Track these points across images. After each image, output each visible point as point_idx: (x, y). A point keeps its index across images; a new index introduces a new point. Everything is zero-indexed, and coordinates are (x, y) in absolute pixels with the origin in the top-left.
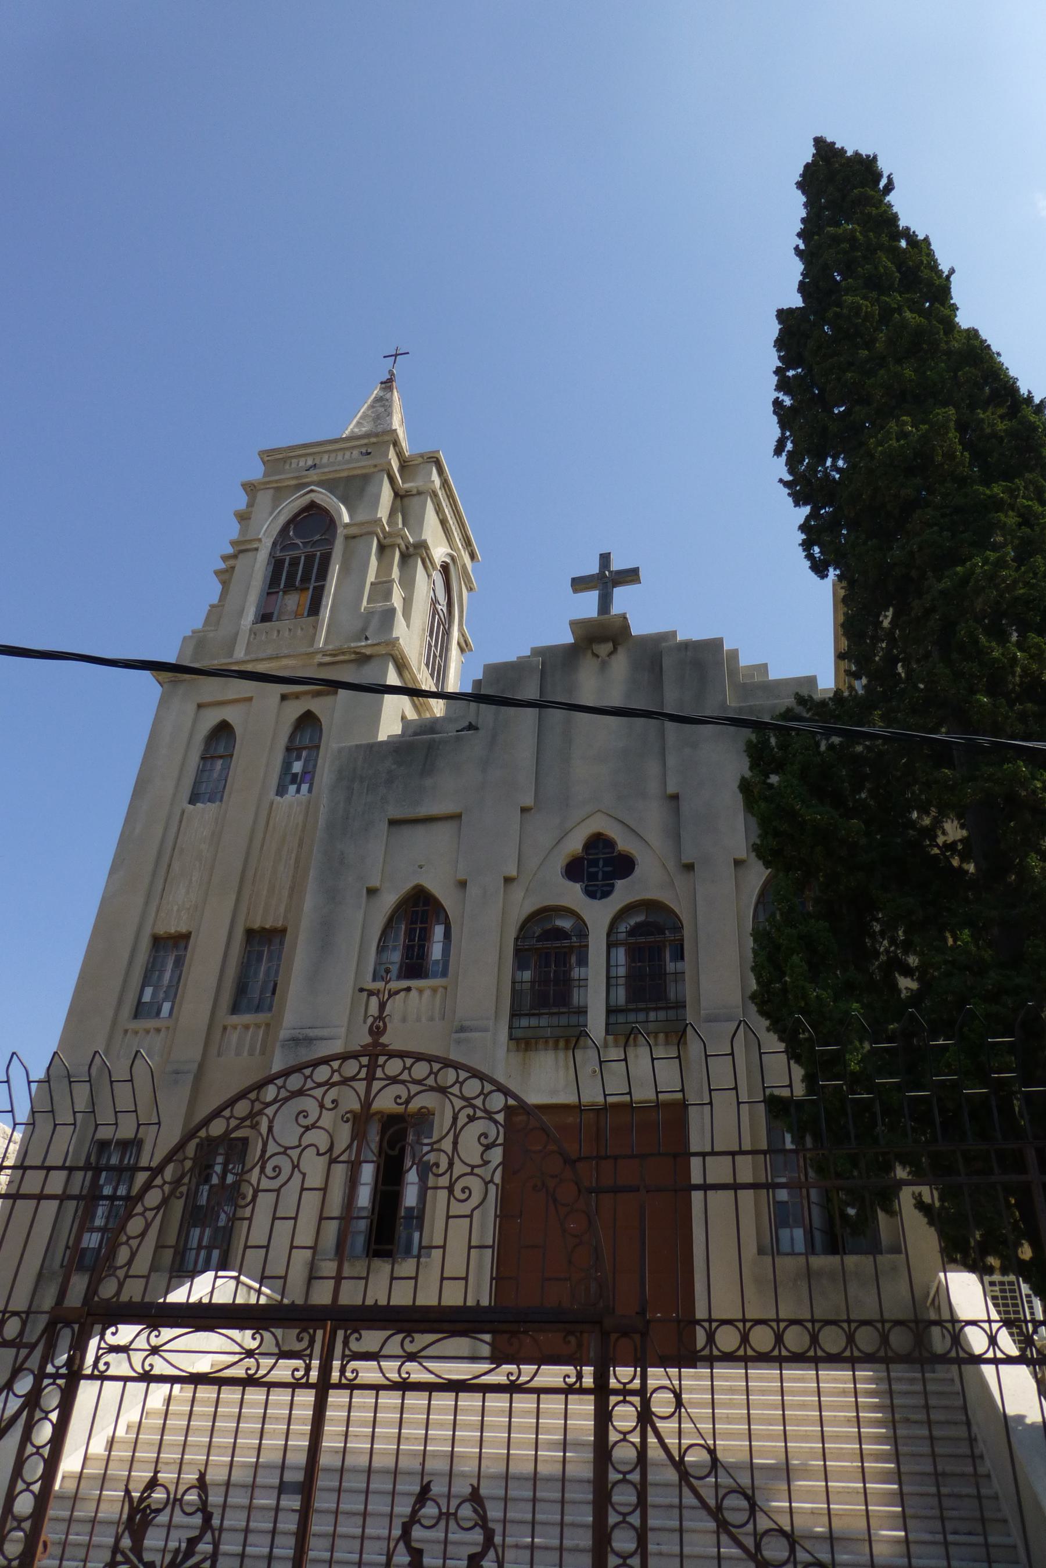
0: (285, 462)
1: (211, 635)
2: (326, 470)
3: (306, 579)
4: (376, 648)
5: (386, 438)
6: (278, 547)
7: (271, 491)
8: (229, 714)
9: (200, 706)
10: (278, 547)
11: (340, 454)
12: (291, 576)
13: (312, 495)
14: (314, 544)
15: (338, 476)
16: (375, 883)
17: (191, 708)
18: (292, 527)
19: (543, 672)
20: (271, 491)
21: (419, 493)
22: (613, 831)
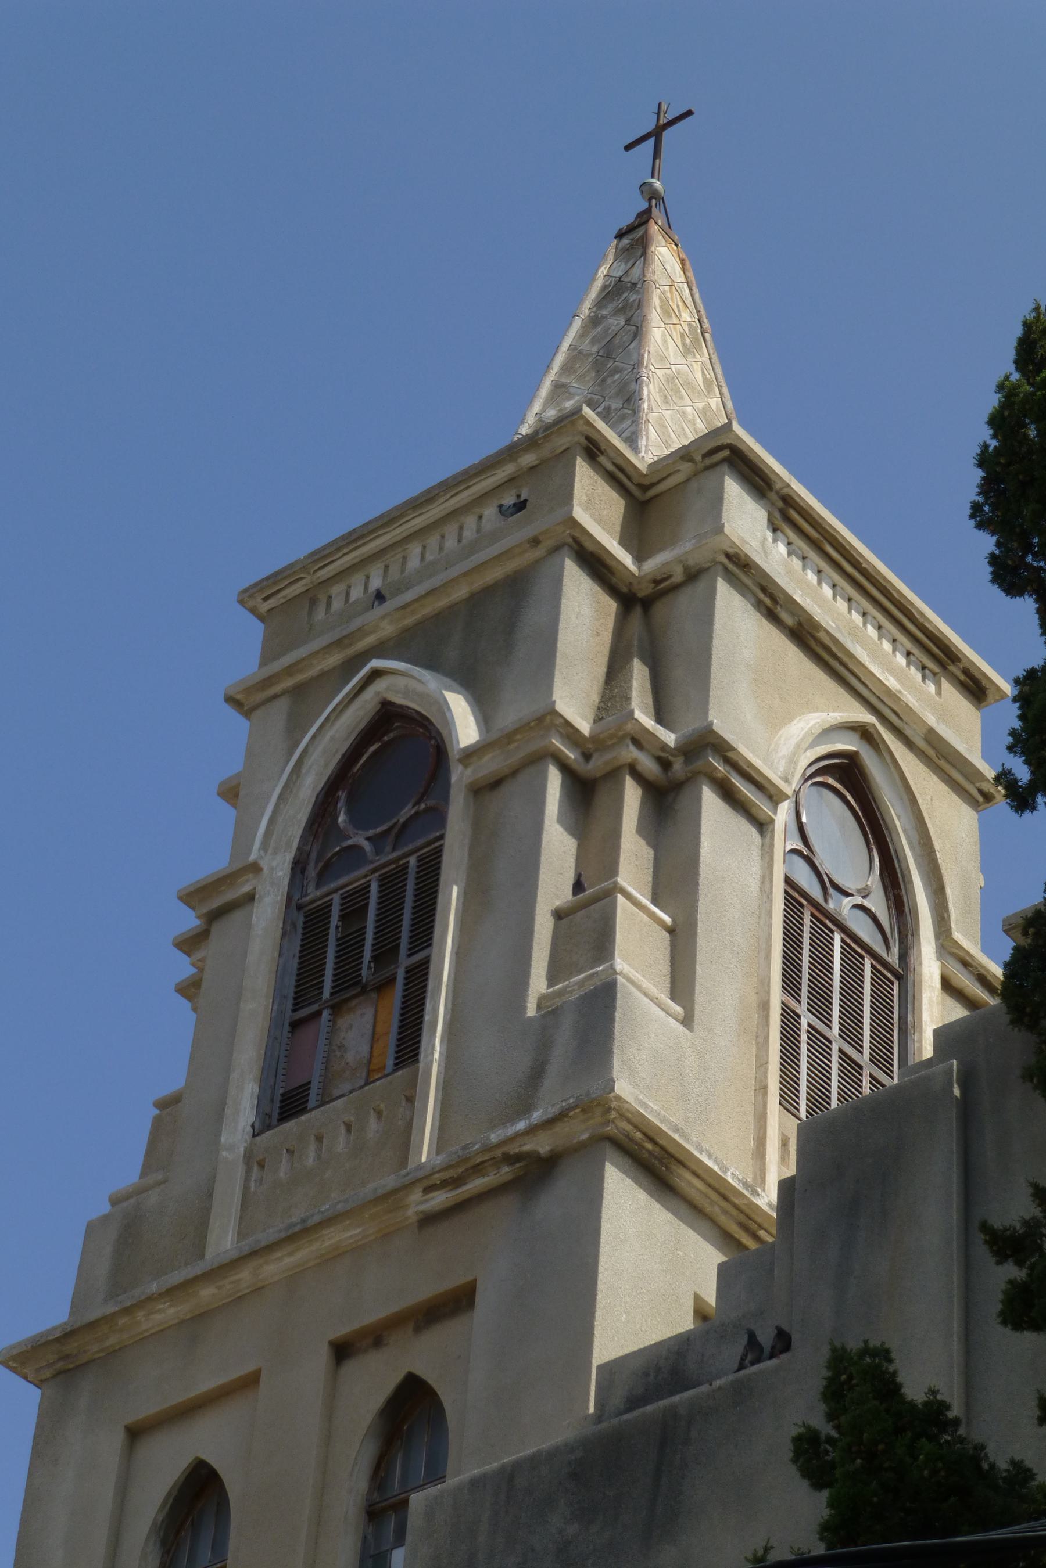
0: (313, 602)
1: (153, 1199)
2: (409, 596)
3: (386, 953)
4: (562, 1129)
5: (561, 442)
6: (312, 872)
7: (283, 705)
8: (209, 1440)
9: (135, 1434)
10: (312, 872)
11: (451, 530)
12: (350, 948)
13: (380, 686)
14: (402, 832)
15: (442, 602)
17: (111, 1442)
18: (342, 795)
19: (967, 1110)
20: (283, 705)
21: (693, 575)
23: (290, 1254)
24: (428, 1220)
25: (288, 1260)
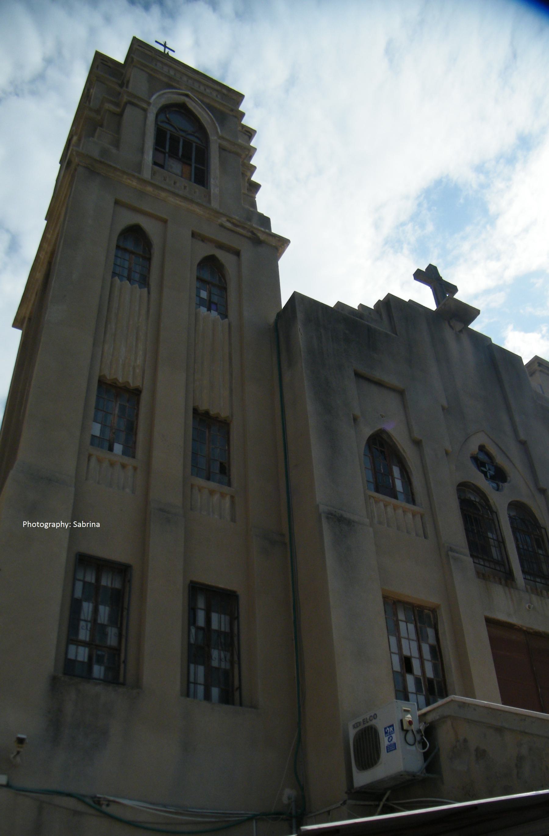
13: (186, 99)
16: (358, 413)
22: (492, 449)
23: (181, 201)
24: (222, 226)
25: (178, 202)
